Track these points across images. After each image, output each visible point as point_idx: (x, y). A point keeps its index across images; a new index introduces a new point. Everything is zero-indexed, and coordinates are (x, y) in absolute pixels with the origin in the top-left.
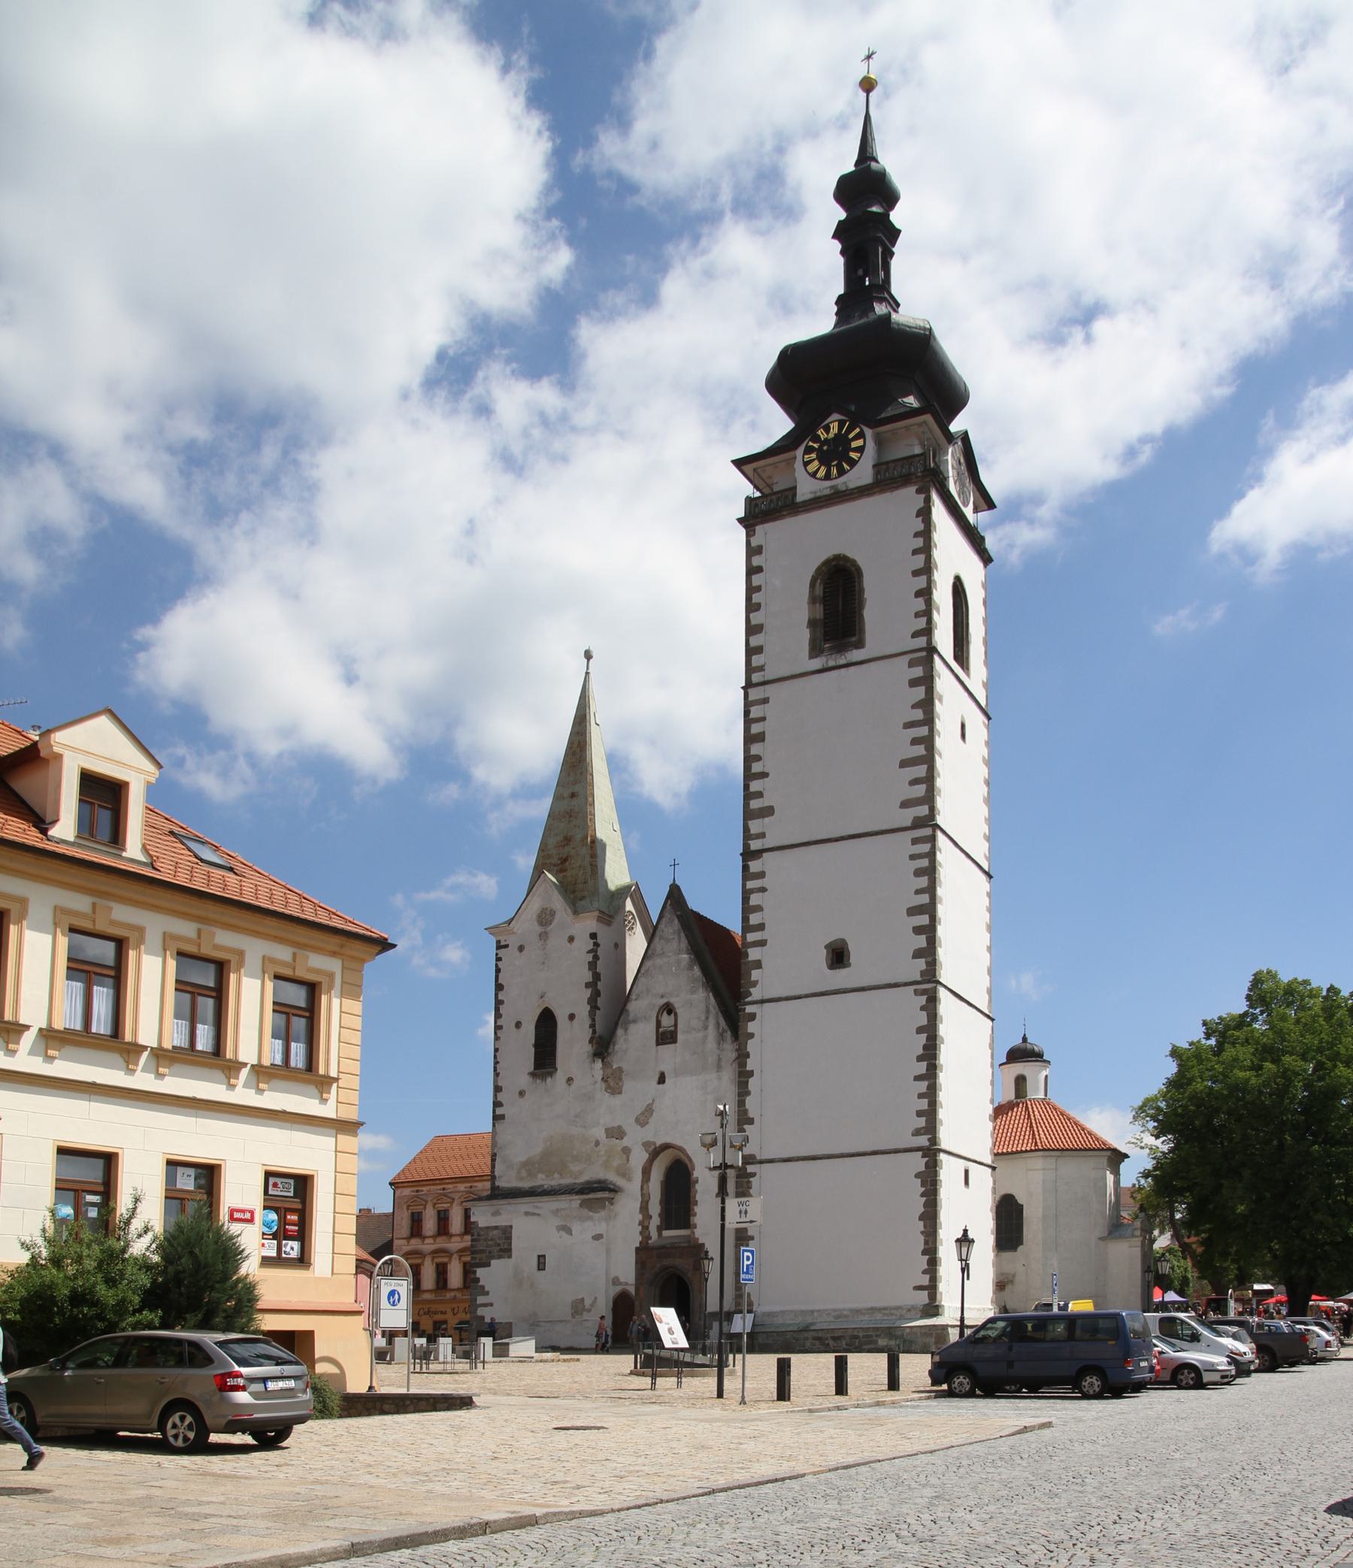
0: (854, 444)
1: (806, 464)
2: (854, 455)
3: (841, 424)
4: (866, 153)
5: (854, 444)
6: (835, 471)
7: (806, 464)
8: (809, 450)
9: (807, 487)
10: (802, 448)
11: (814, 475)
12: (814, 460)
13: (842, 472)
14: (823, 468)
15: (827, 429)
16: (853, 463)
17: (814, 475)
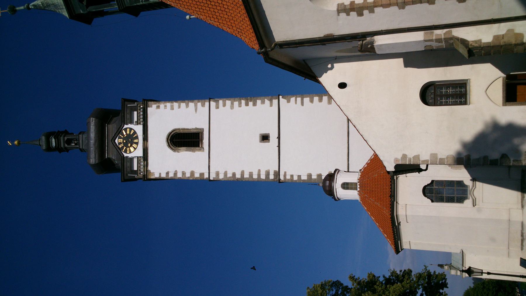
0: (128, 133)
1: (130, 152)
2: (132, 133)
3: (120, 138)
5: (128, 133)
6: (136, 141)
7: (130, 152)
8: (126, 151)
10: (125, 155)
11: (135, 149)
12: (130, 149)
13: (137, 138)
14: (133, 145)
15: (120, 143)
16: (135, 133)
17: (135, 149)
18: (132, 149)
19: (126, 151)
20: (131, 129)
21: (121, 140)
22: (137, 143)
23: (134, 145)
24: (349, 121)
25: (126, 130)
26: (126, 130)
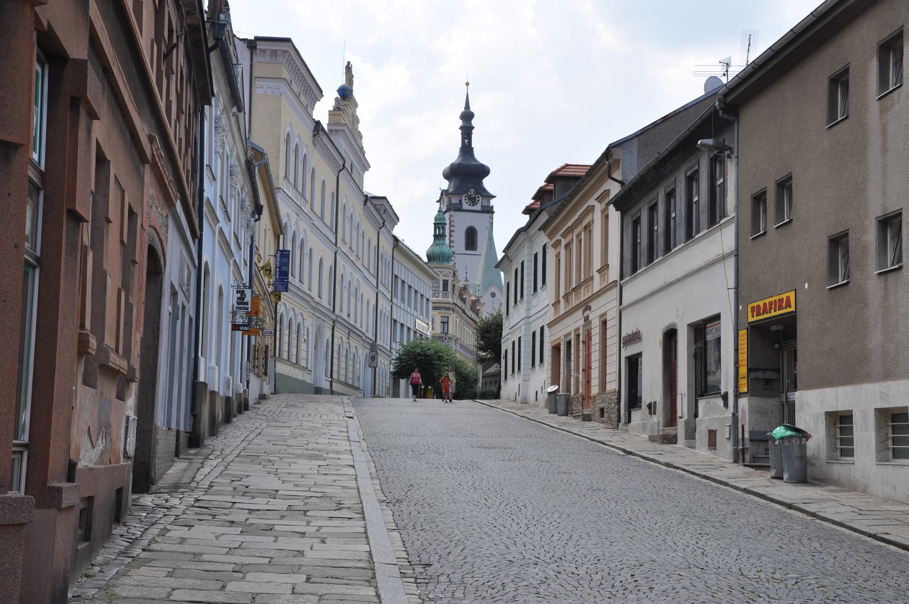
1: (465, 200)
3: (474, 192)
4: (467, 106)
8: (466, 196)
9: (465, 206)
10: (464, 196)
13: (474, 205)
15: (470, 192)
16: (477, 204)
18: (467, 201)
19: (466, 196)
20: (478, 201)
21: (472, 193)
22: (470, 205)
23: (469, 203)
24: (334, 232)
25: (478, 197)
26: (478, 197)
